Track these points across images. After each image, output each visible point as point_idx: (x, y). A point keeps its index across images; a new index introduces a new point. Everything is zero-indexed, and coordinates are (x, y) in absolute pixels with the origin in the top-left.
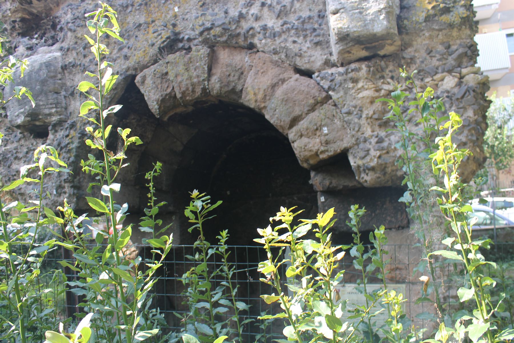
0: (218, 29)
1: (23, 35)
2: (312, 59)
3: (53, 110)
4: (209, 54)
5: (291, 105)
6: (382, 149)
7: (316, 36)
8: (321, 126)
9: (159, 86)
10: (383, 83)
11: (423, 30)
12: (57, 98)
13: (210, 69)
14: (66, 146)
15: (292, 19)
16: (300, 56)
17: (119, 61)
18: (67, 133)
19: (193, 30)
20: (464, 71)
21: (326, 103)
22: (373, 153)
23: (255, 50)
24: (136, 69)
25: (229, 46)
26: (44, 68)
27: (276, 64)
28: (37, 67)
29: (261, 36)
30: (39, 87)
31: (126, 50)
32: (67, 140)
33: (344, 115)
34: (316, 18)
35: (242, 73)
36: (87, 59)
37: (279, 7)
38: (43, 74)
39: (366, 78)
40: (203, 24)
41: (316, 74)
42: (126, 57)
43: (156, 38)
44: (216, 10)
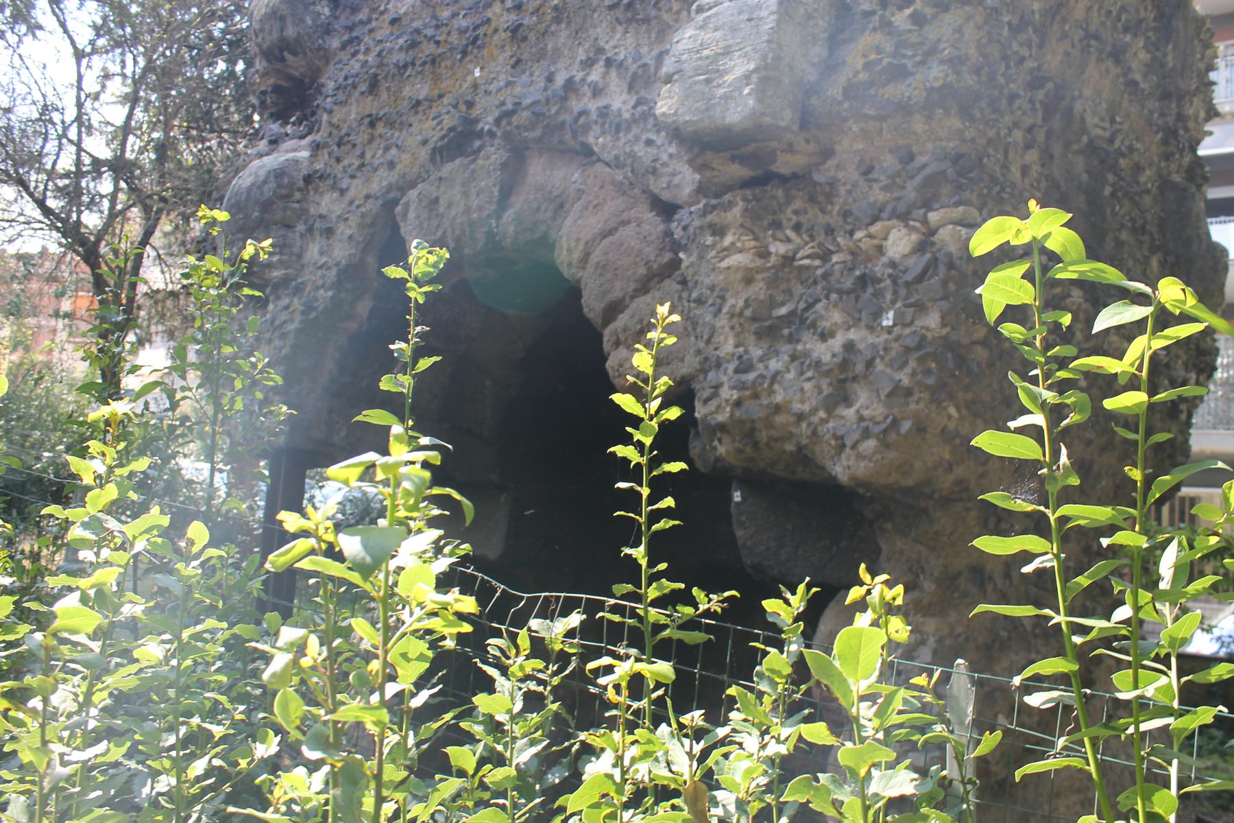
0: (525, 114)
2: (676, 180)
4: (504, 166)
5: (609, 276)
9: (425, 225)
10: (775, 238)
11: (845, 120)
12: (284, 236)
13: (506, 194)
20: (933, 217)
21: (669, 277)
23: (594, 158)
26: (272, 179)
27: (621, 190)
28: (261, 178)
30: (257, 214)
31: (394, 151)
33: (692, 305)
35: (561, 206)
36: (340, 167)
37: (633, 68)
38: (268, 191)
39: (742, 226)
42: (391, 165)
43: (434, 129)
44: (537, 74)
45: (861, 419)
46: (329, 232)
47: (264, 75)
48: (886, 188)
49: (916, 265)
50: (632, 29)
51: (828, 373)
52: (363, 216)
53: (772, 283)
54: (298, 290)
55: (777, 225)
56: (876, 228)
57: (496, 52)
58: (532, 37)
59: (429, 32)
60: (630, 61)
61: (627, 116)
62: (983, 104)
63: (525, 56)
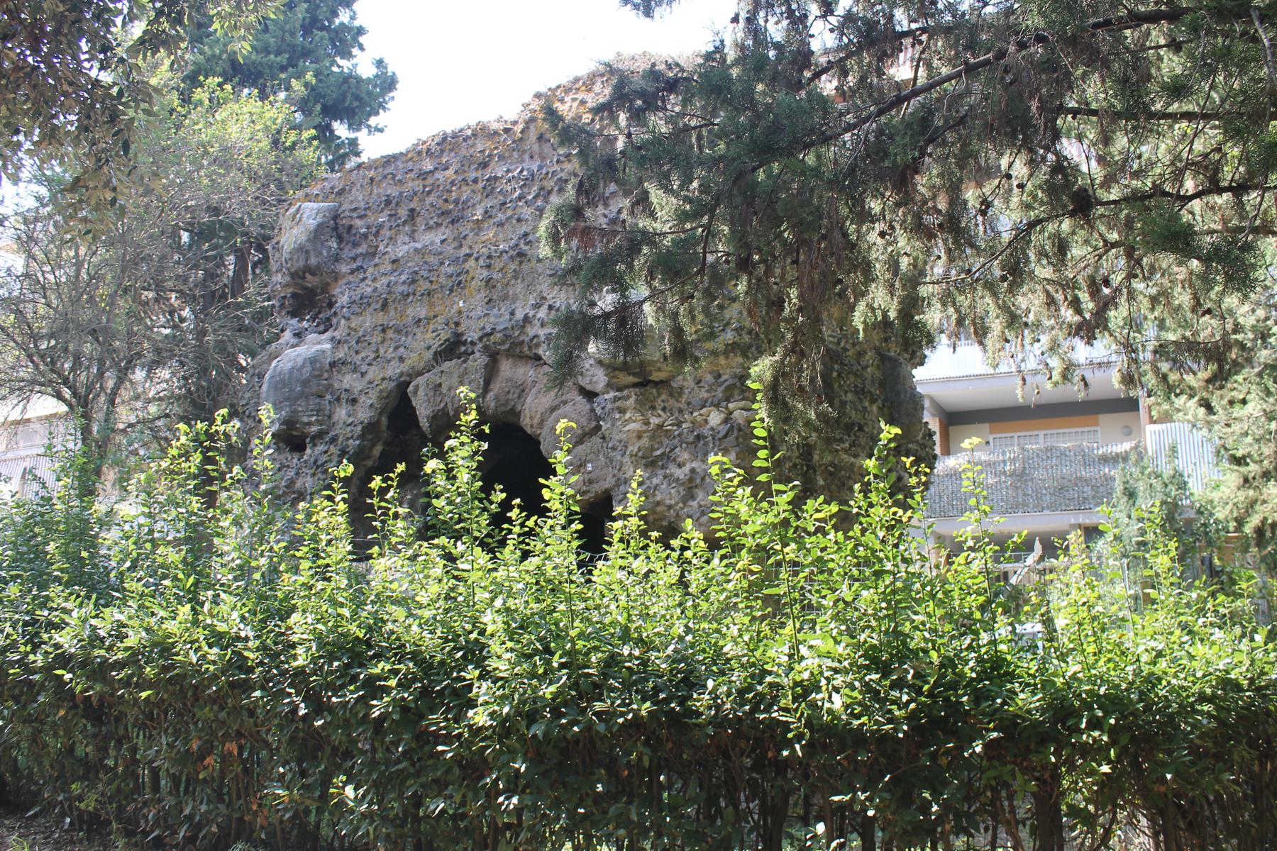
0: (499, 335)
1: (293, 314)
2: (595, 379)
3: (314, 419)
4: (486, 366)
14: (323, 465)
20: (731, 406)
24: (410, 375)
25: (514, 356)
28: (300, 364)
31: (402, 350)
32: (324, 458)
35: (523, 391)
36: (359, 357)
38: (307, 372)
40: (484, 328)
42: (401, 359)
45: (700, 506)
46: (354, 401)
48: (708, 391)
49: (724, 429)
51: (683, 484)
52: (381, 391)
53: (652, 438)
54: (334, 440)
55: (653, 408)
56: (704, 411)
59: (425, 274)
62: (753, 349)
63: (495, 297)
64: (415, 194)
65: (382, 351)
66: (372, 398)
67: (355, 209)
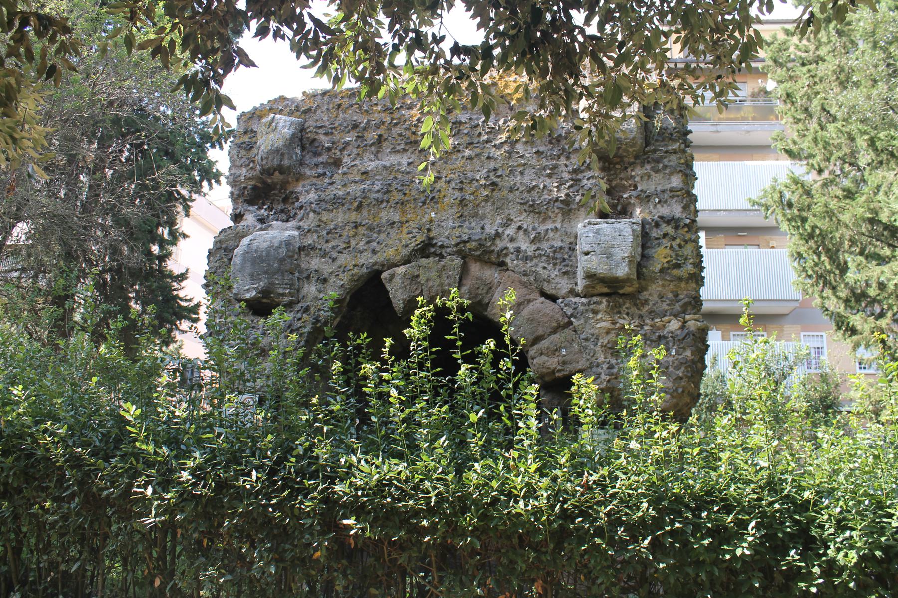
0: (474, 243)
2: (559, 286)
3: (287, 291)
6: (612, 374)
7: (564, 266)
8: (561, 348)
10: (619, 318)
13: (461, 279)
14: (298, 329)
15: (545, 245)
16: (549, 281)
17: (366, 253)
18: (299, 315)
19: (448, 238)
20: (688, 317)
22: (603, 376)
24: (383, 265)
27: (524, 284)
28: (276, 244)
29: (513, 257)
31: (374, 244)
32: (299, 324)
34: (567, 250)
35: (491, 288)
38: (283, 251)
41: (560, 300)
42: (374, 252)
44: (473, 224)
46: (325, 280)
47: (248, 179)
50: (532, 215)
52: (353, 275)
54: (306, 310)
57: (446, 208)
58: (471, 206)
60: (530, 229)
61: (529, 253)
64: (383, 123)
65: (353, 243)
66: (345, 278)
67: (321, 127)
